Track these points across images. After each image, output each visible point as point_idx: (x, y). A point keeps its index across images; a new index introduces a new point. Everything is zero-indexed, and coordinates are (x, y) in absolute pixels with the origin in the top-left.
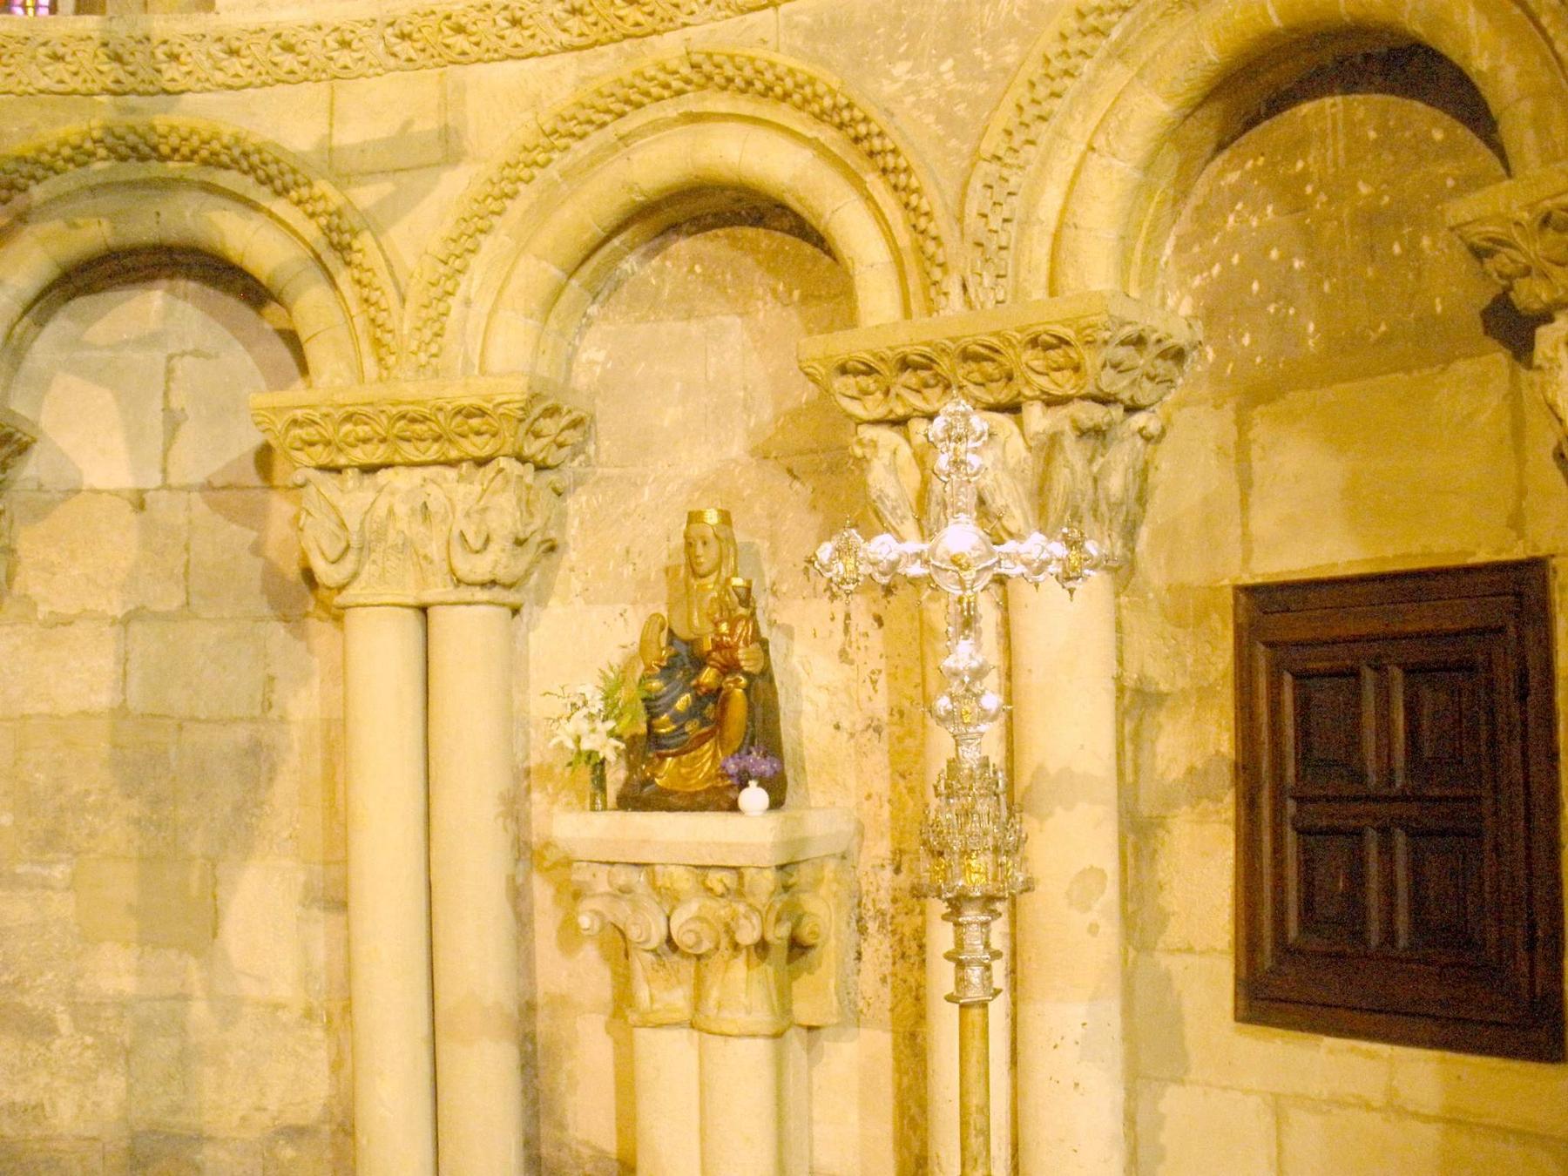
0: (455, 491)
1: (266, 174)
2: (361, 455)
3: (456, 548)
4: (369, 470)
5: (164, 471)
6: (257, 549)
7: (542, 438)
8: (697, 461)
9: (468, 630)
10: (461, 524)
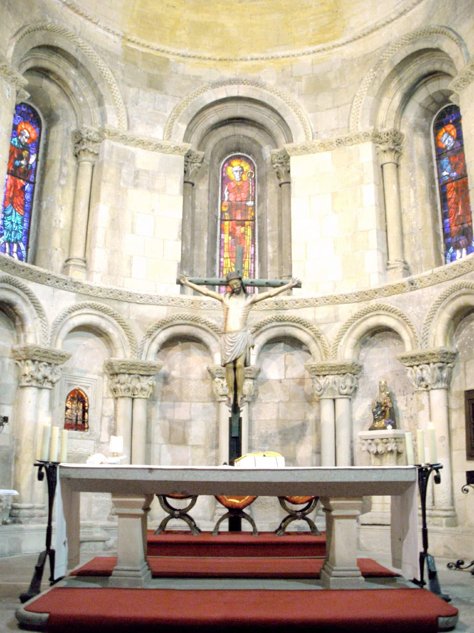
0: (338, 378)
2: (324, 373)
3: (341, 389)
4: (324, 376)
5: (285, 376)
6: (303, 390)
7: (355, 370)
8: (381, 372)
9: (342, 404)
10: (341, 384)
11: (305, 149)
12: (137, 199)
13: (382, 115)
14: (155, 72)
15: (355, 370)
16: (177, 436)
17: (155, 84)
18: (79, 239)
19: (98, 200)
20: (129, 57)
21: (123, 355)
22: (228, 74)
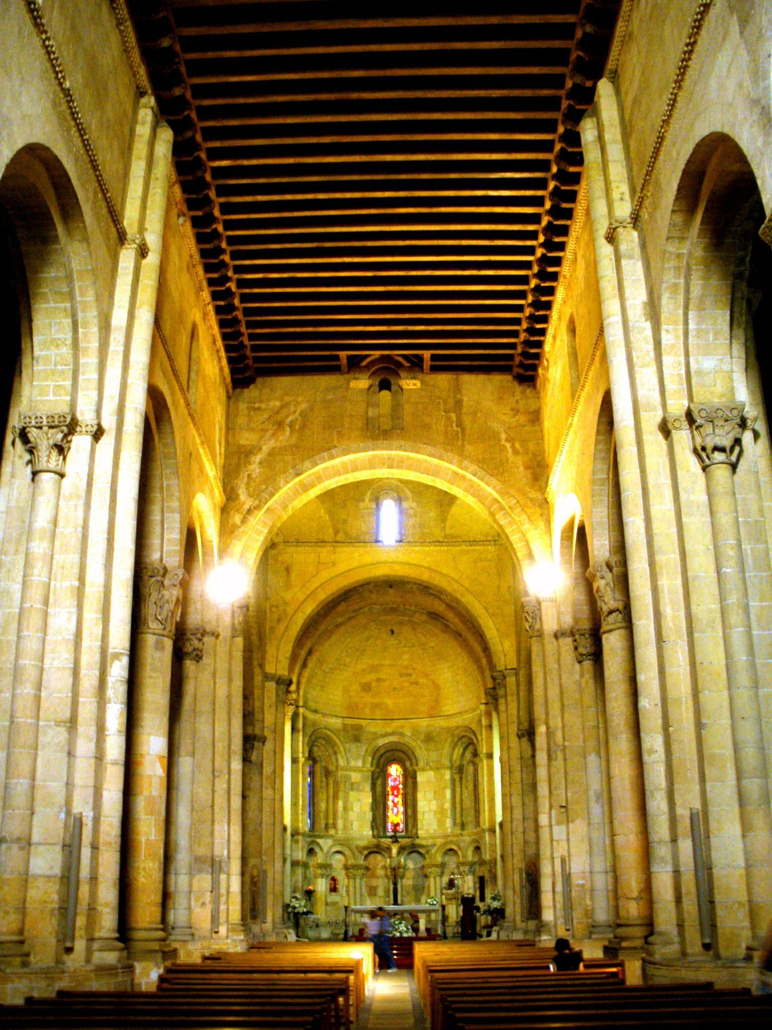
1: (423, 846)
7: (443, 866)
11: (423, 770)
12: (353, 795)
13: (455, 757)
14: (356, 733)
15: (443, 866)
16: (372, 891)
17: (357, 739)
18: (331, 815)
19: (338, 799)
20: (345, 727)
21: (351, 862)
22: (389, 730)
